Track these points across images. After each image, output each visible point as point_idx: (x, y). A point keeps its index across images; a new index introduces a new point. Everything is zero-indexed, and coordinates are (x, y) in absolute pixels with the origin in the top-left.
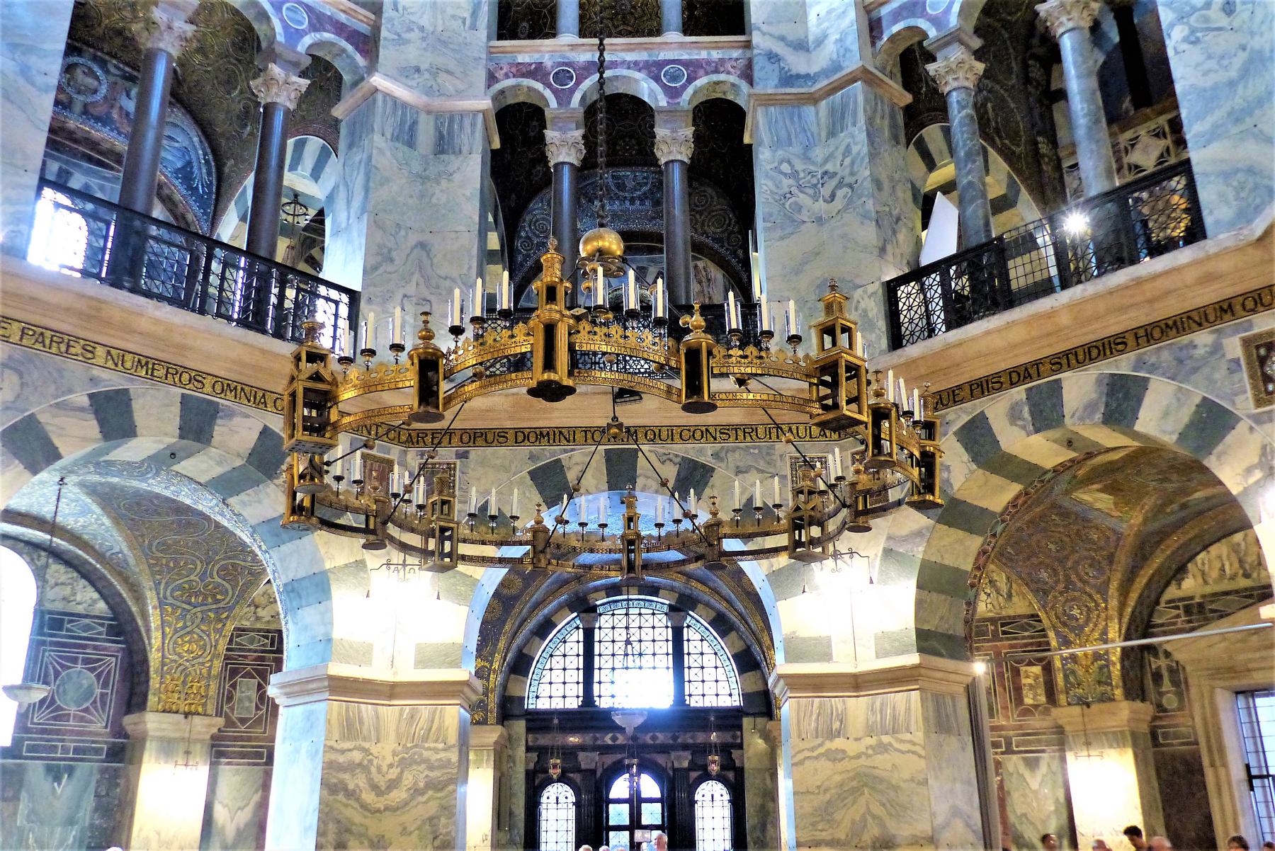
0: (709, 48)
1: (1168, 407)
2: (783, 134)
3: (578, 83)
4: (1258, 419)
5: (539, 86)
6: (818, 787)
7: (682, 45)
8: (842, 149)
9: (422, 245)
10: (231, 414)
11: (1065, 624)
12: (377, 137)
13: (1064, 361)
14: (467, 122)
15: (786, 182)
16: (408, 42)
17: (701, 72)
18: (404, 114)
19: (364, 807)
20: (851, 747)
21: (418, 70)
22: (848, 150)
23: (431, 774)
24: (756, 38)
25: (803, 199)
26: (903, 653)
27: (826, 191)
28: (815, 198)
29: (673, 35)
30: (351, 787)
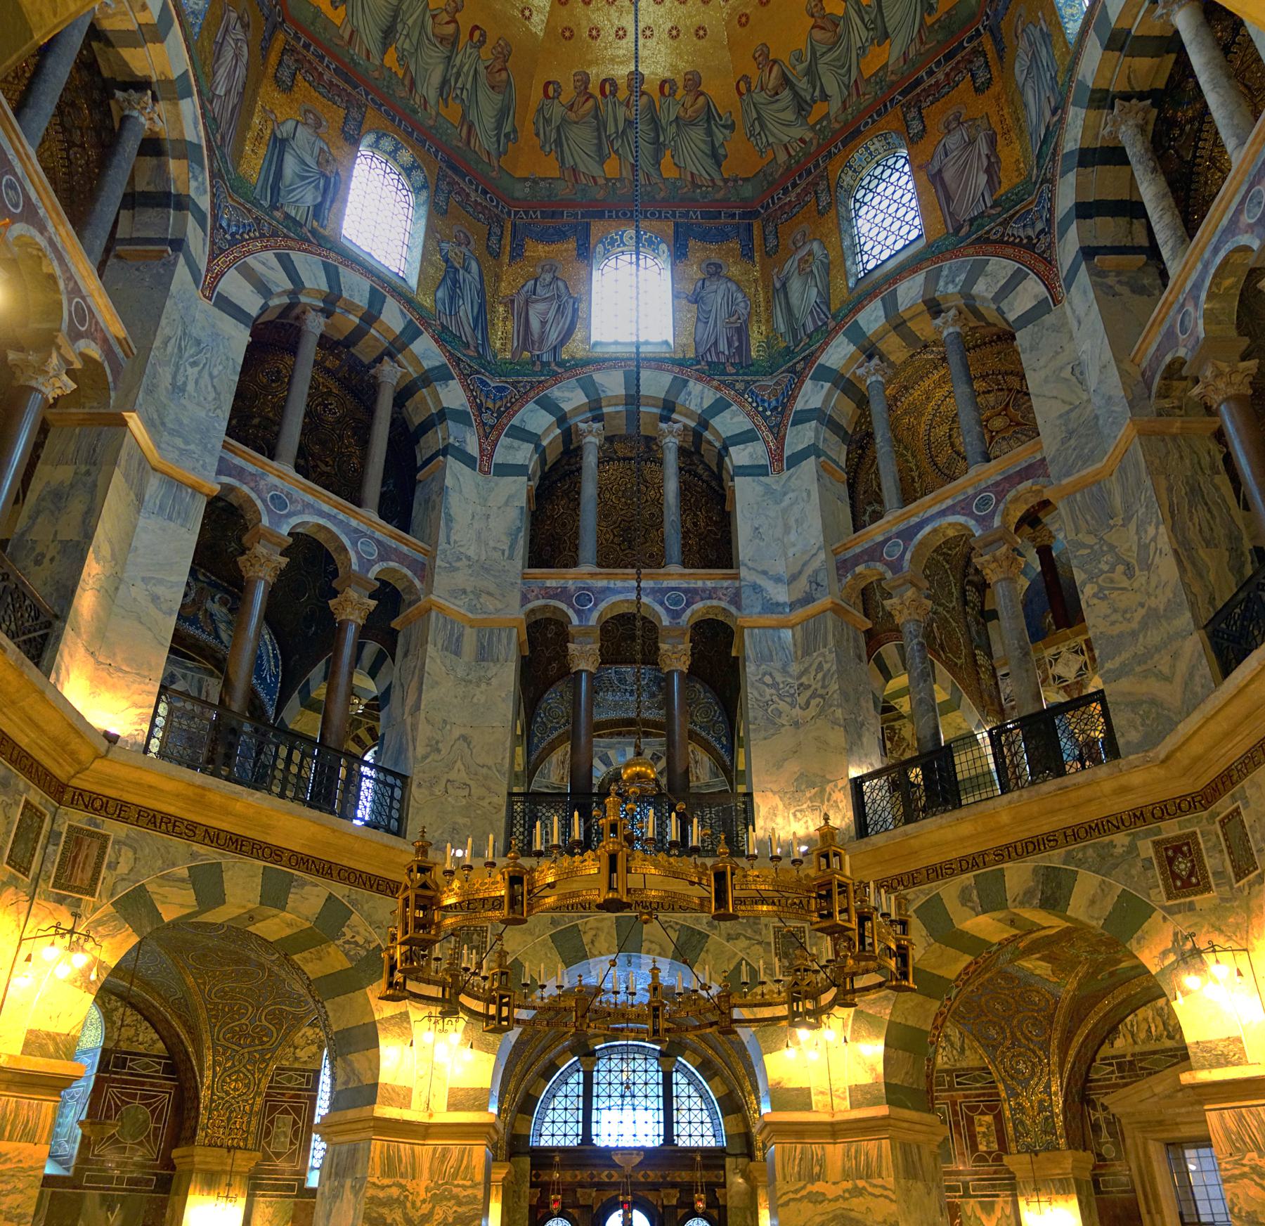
0: (704, 579)
1: (1094, 896)
2: (766, 651)
3: (596, 605)
4: (1170, 911)
5: (563, 606)
7: (682, 575)
8: (815, 666)
9: (464, 738)
10: (303, 884)
11: (1012, 1078)
12: (430, 648)
13: (1006, 854)
14: (504, 635)
15: (768, 691)
16: (458, 569)
17: (698, 598)
18: (453, 629)
21: (464, 592)
22: (820, 667)
24: (743, 572)
25: (782, 705)
26: (874, 1104)
27: (801, 700)
28: (793, 705)
29: (675, 569)
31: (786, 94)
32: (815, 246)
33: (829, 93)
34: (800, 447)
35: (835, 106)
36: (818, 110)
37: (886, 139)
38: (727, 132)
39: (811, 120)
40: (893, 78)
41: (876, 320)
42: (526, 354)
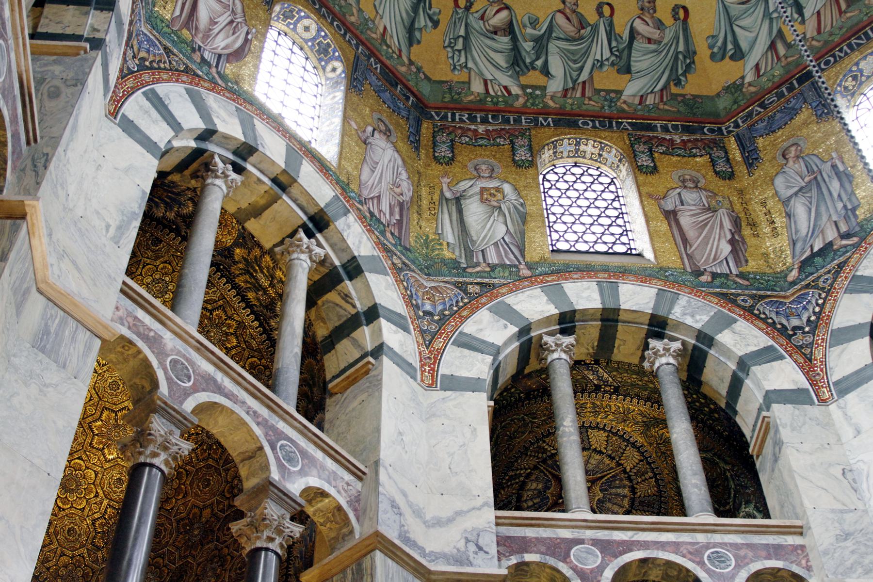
31: (504, 41)
32: (507, 188)
33: (552, 71)
34: (465, 373)
35: (555, 86)
36: (534, 78)
37: (602, 149)
38: (430, 24)
39: (524, 80)
40: (625, 106)
41: (588, 299)
42: (185, 33)
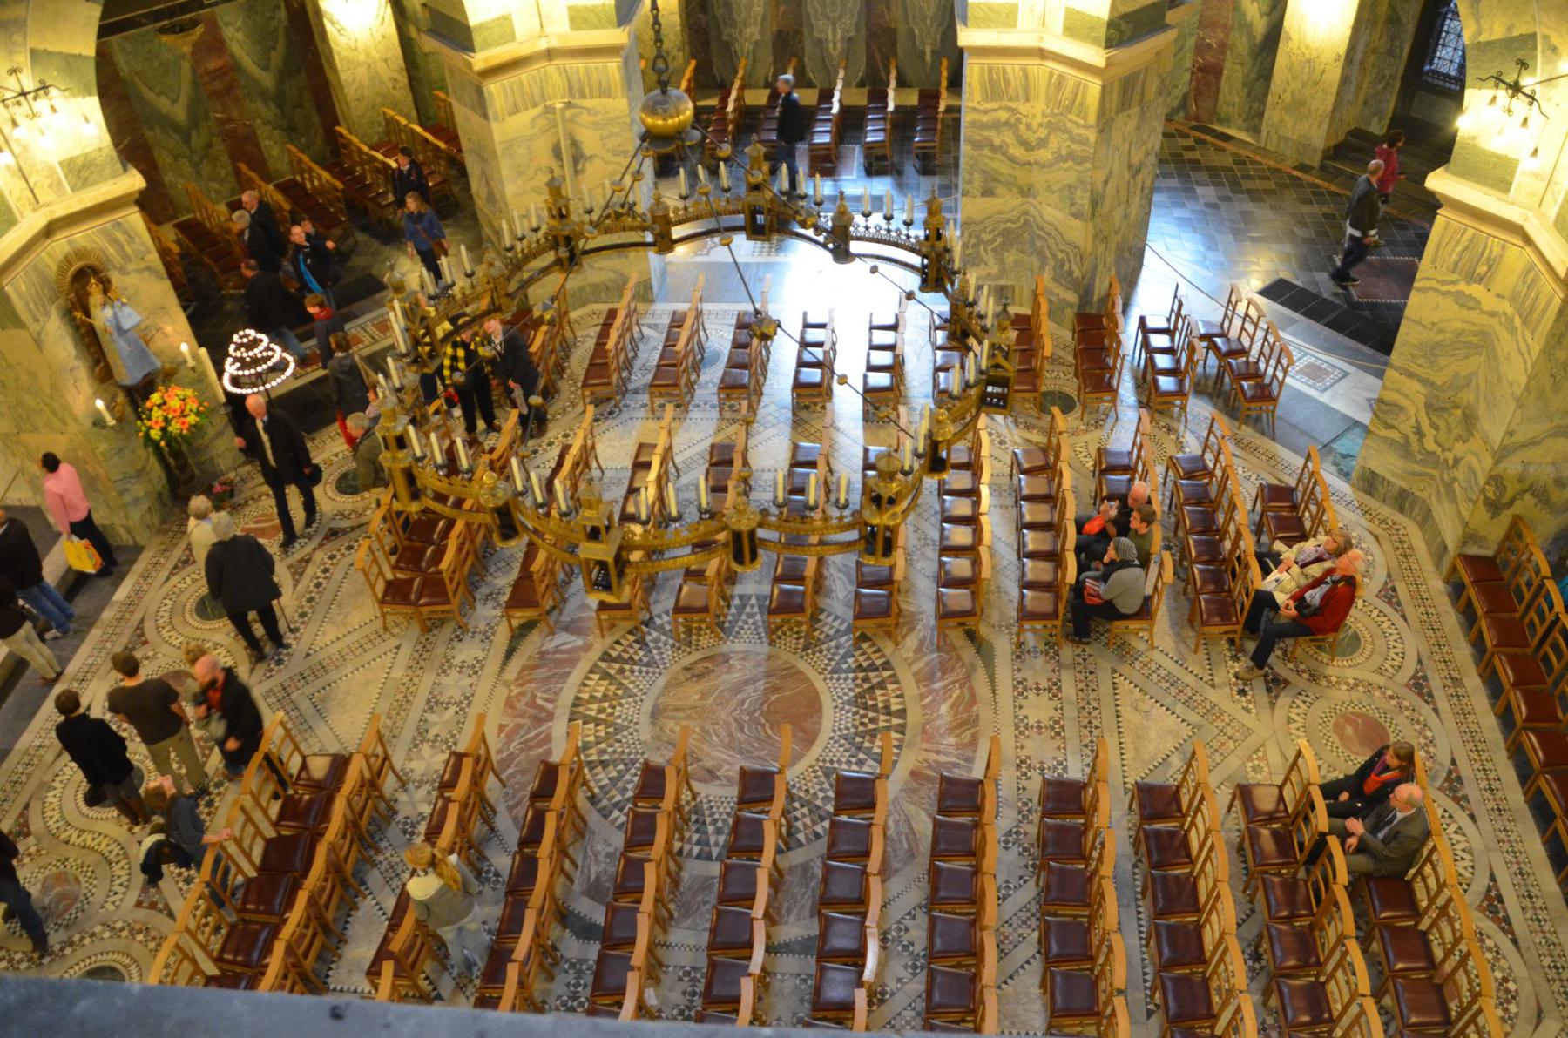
6: (1433, 324)
19: (1012, 160)
20: (1488, 301)
23: (1074, 147)
30: (997, 142)
